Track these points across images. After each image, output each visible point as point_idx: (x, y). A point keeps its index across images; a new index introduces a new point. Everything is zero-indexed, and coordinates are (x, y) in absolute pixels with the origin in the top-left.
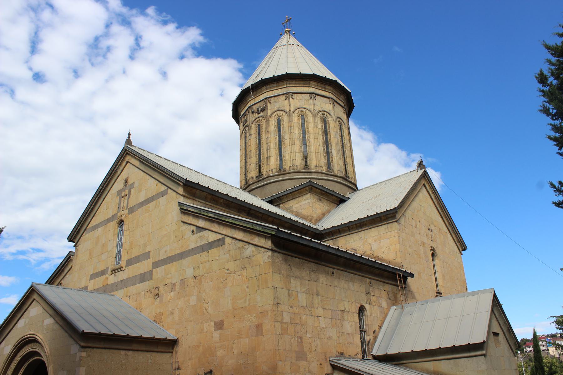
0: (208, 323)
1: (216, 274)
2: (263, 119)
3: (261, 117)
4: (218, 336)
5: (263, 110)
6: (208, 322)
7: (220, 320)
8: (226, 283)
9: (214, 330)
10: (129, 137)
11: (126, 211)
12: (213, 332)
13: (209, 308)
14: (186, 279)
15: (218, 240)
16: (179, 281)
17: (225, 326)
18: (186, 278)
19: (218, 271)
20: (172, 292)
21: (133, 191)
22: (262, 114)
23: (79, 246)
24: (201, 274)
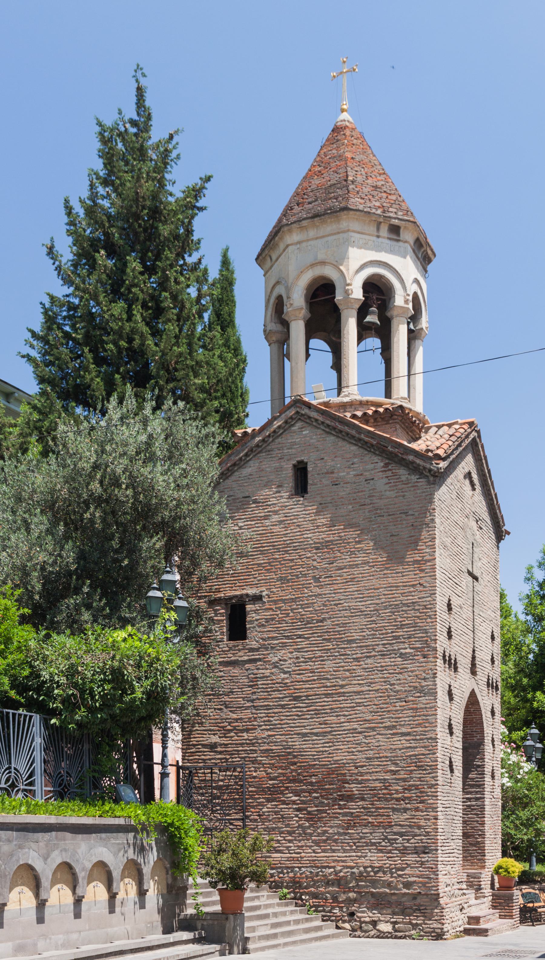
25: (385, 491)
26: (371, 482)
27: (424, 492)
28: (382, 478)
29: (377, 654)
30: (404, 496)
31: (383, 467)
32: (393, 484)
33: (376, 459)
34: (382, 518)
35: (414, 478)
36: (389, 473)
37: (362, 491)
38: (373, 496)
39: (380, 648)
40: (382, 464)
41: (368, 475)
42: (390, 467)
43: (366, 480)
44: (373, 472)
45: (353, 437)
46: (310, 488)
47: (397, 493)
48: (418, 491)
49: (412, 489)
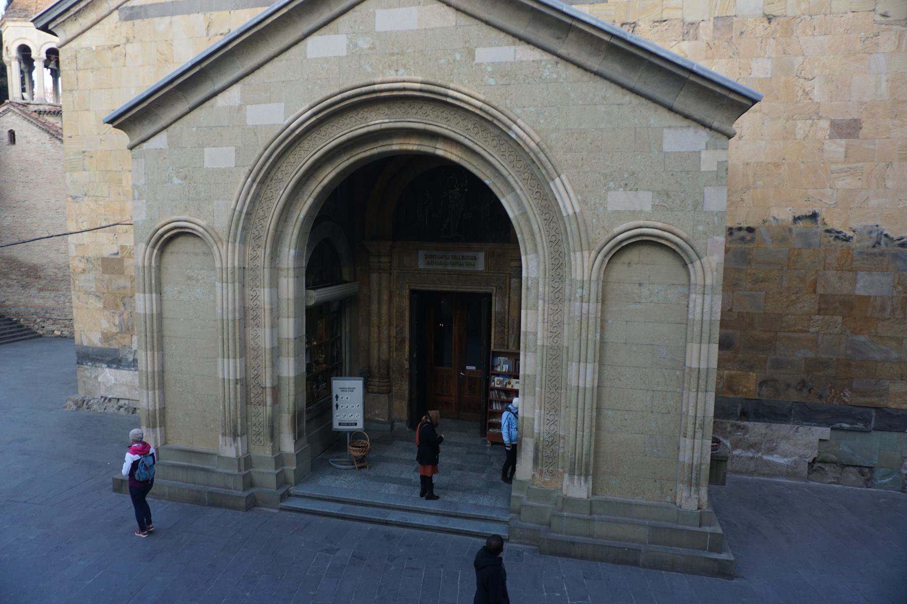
0: (810, 122)
1: (843, 19)
4: (843, 150)
6: (810, 119)
7: (851, 118)
8: (877, 45)
9: (827, 137)
12: (827, 142)
13: (816, 91)
14: (734, 18)
16: (712, 19)
17: (862, 133)
18: (735, 16)
19: (853, 14)
20: (684, 40)
24: (790, 13)
33: (46, 135)
39: (51, 216)
41: (43, 141)
46: (16, 142)
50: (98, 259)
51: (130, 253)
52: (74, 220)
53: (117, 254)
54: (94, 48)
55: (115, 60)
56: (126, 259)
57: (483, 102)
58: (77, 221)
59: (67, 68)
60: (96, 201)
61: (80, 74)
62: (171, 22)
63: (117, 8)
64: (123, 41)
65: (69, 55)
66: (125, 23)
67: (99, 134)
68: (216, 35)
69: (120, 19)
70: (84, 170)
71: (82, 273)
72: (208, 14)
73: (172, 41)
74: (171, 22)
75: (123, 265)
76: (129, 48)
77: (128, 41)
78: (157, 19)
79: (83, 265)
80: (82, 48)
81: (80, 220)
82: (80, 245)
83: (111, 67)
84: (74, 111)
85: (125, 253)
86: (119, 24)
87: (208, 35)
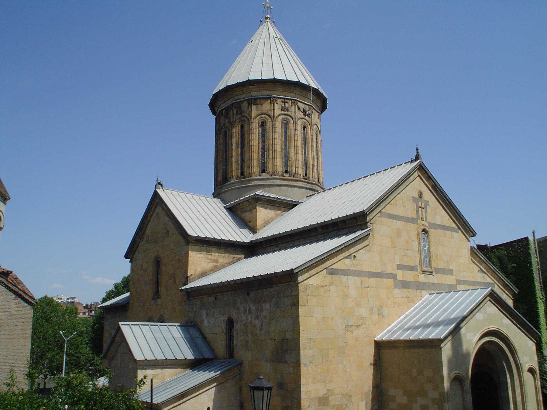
2: (308, 124)
3: (307, 121)
5: (309, 115)
10: (417, 152)
11: (427, 224)
15: (492, 283)
21: (428, 208)
22: (306, 117)
23: (374, 225)
25: (15, 307)
26: (9, 303)
27: (29, 311)
28: (14, 302)
29: (5, 372)
30: (21, 311)
31: (15, 298)
32: (17, 305)
33: (12, 294)
34: (12, 318)
35: (26, 304)
36: (17, 301)
37: (5, 306)
38: (9, 309)
40: (14, 297)
41: (8, 300)
42: (17, 299)
43: (7, 302)
44: (10, 299)
45: (5, 284)
47: (19, 309)
48: (27, 310)
49: (25, 309)
50: (316, 398)
51: (332, 393)
52: (305, 377)
53: (326, 394)
54: (315, 285)
55: (325, 292)
56: (330, 397)
57: (506, 334)
58: (306, 378)
59: (302, 294)
60: (316, 366)
61: (309, 298)
62: (347, 279)
63: (325, 269)
64: (328, 284)
65: (303, 287)
66: (329, 275)
67: (317, 329)
68: (364, 287)
69: (327, 273)
70: (310, 349)
71: (308, 408)
72: (361, 278)
73: (348, 287)
74: (347, 279)
75: (329, 400)
76: (333, 288)
77: (330, 285)
78: (342, 276)
79: (309, 403)
80: (309, 285)
81: (308, 377)
82: (308, 391)
83: (323, 296)
84: (306, 317)
85: (329, 393)
86: (326, 275)
87: (361, 287)
